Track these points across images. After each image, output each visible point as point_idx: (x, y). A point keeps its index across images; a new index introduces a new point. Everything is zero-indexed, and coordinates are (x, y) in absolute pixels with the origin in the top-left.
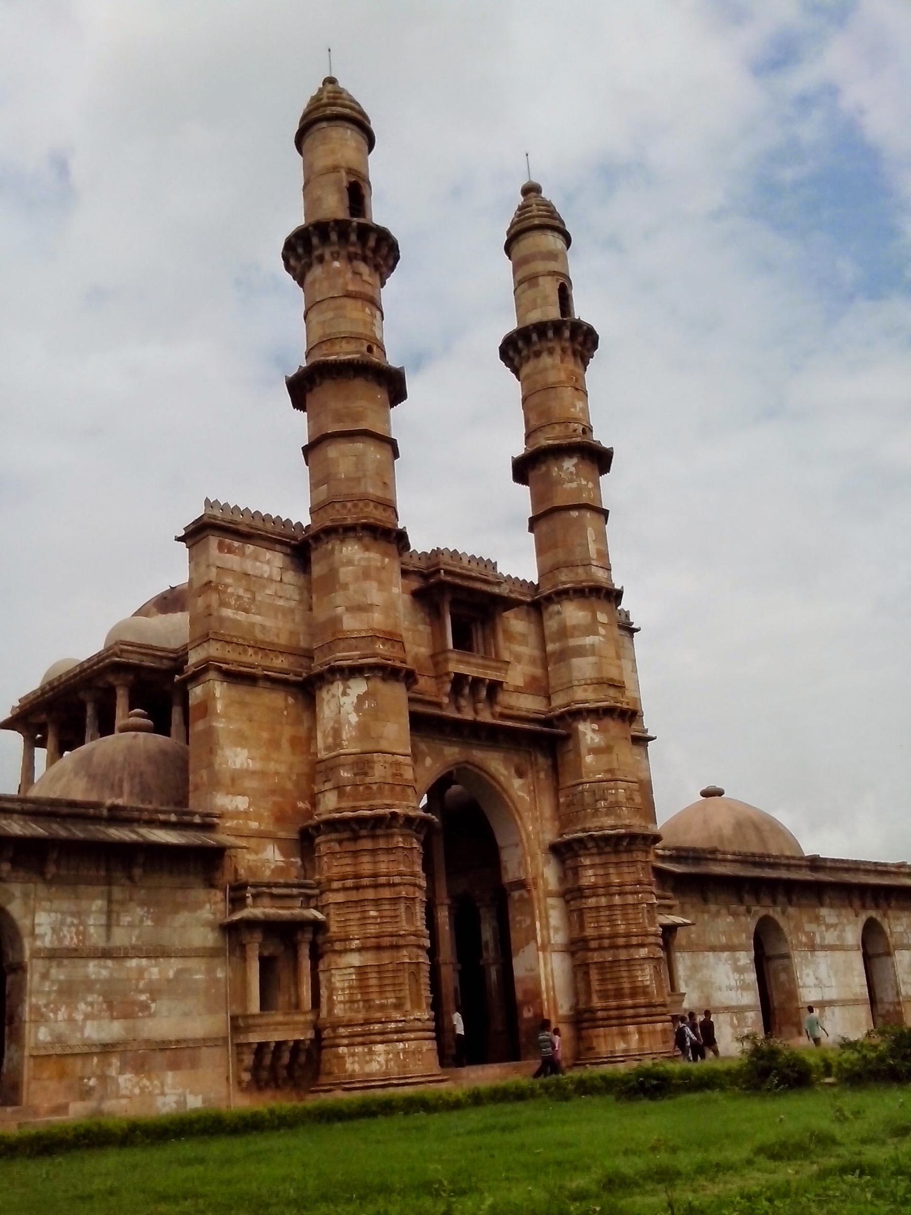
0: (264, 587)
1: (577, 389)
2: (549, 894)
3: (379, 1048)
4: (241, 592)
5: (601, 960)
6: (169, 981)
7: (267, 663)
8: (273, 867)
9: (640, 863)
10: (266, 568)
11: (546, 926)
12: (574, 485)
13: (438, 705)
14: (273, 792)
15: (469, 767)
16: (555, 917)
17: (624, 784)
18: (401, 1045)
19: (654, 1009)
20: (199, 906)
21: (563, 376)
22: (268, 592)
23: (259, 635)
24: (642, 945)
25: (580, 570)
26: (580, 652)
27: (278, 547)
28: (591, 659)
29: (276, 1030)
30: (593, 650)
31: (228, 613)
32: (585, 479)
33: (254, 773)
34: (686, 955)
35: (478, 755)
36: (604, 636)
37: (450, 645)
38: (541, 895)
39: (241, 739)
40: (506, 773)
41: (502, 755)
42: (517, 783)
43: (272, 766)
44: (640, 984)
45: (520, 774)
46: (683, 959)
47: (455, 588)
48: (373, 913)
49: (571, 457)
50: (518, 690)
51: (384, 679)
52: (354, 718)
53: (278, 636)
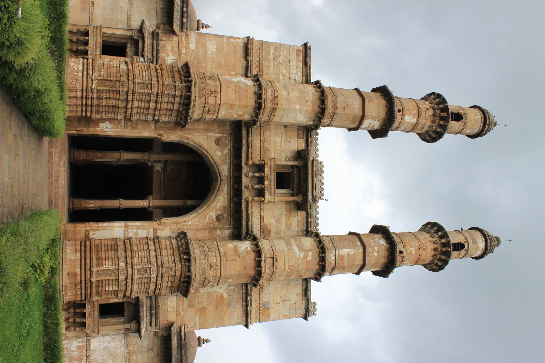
0: (286, 70)
1: (420, 249)
2: (155, 230)
3: (81, 67)
4: (282, 58)
5: (119, 249)
6: (118, 3)
7: (254, 66)
8: (166, 58)
9: (174, 265)
10: (294, 72)
11: (138, 228)
12: (373, 244)
13: (247, 159)
14: (199, 63)
15: (219, 182)
16: (142, 234)
17: (219, 263)
18: (81, 74)
19: (88, 267)
20: (149, 21)
21: (423, 242)
22: (284, 71)
23: (265, 64)
24: (126, 266)
25: (331, 245)
26: (288, 243)
27: (304, 78)
28: (285, 248)
29: (94, 40)
30: (290, 249)
31: (272, 51)
32: (378, 249)
33: (206, 53)
34: (123, 349)
36: (299, 256)
37: (277, 163)
38: (154, 227)
39: (220, 49)
40: (218, 207)
41: (226, 204)
42: (213, 215)
43: (210, 63)
44: (104, 263)
45: (218, 218)
46: (120, 347)
47: (306, 166)
48: (144, 73)
49: (386, 243)
50: (262, 218)
51: (255, 93)
52: (235, 80)
53: (266, 74)
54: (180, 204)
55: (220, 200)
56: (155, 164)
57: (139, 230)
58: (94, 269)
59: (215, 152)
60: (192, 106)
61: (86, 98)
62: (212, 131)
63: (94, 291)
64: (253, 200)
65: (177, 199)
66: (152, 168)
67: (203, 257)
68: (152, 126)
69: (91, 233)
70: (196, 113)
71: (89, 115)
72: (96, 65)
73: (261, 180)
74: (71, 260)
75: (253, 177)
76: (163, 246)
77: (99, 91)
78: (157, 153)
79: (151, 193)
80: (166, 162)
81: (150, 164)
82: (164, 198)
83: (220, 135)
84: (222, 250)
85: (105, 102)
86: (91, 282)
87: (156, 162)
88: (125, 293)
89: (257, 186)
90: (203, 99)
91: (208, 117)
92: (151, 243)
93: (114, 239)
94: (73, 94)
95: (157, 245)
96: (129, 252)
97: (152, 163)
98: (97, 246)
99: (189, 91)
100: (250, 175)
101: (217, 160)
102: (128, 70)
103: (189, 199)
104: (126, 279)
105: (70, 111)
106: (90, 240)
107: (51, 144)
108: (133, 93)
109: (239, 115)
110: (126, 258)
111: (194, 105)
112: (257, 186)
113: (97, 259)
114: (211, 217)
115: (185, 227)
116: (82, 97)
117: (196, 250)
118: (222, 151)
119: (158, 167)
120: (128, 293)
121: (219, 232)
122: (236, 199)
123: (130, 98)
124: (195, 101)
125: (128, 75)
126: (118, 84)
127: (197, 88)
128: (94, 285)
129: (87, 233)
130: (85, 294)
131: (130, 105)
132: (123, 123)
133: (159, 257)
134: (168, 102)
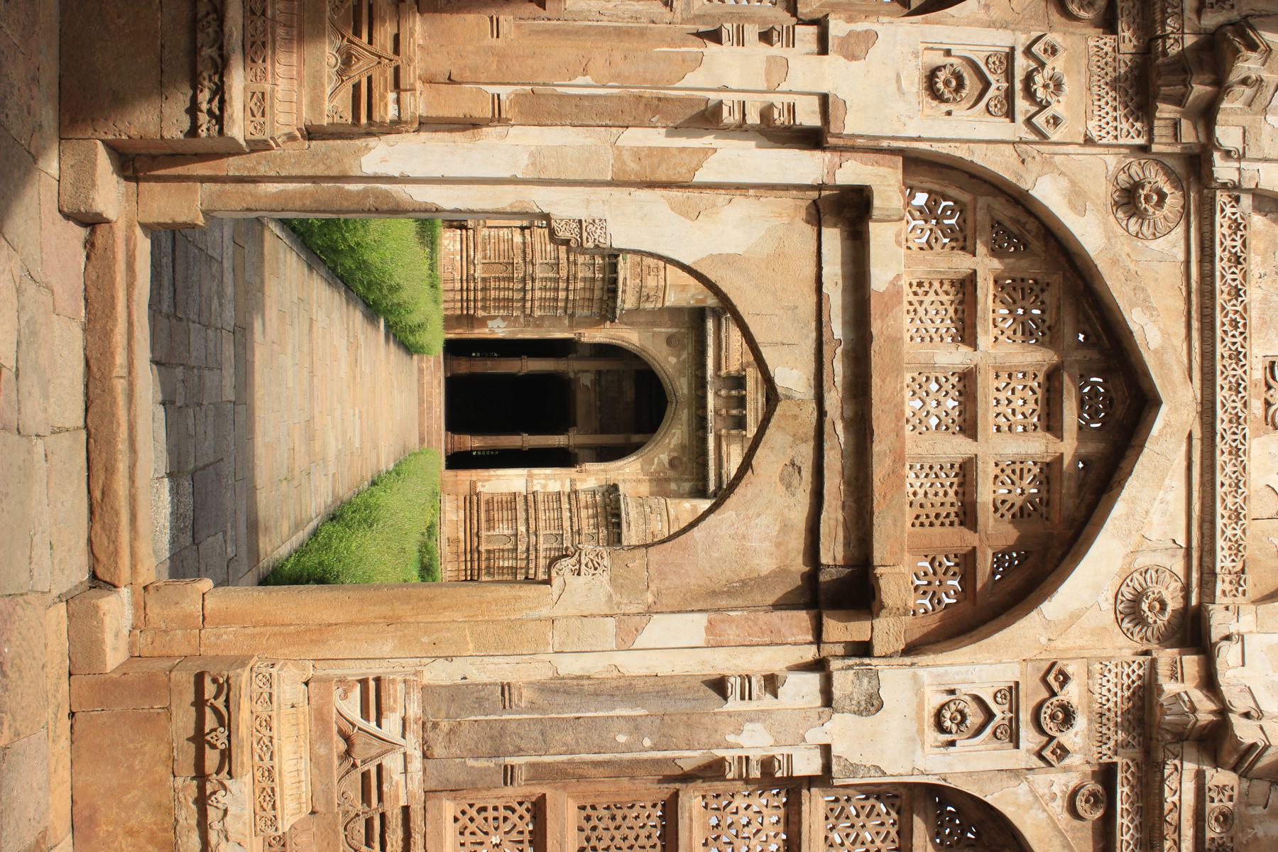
11: (547, 477)
16: (554, 487)
18: (458, 258)
24: (528, 530)
35: (684, 415)
42: (665, 458)
45: (672, 463)
54: (619, 441)
55: (674, 436)
56: (580, 375)
57: (549, 480)
58: (483, 533)
59: (666, 358)
60: (620, 293)
61: (468, 289)
62: (660, 325)
63: (483, 565)
64: (729, 435)
65: (618, 433)
66: (577, 380)
67: (641, 521)
68: (566, 322)
69: (479, 484)
70: (627, 300)
71: (472, 312)
72: (479, 240)
73: (741, 402)
74: (451, 521)
75: (729, 397)
76: (582, 504)
77: (484, 280)
78: (583, 358)
79: (575, 425)
80: (599, 373)
81: (572, 375)
82: (596, 433)
83: (675, 330)
84: (672, 511)
85: (493, 294)
86: (479, 552)
87: (582, 372)
88: (527, 573)
89: (734, 412)
90: (638, 281)
91: (649, 306)
92: (564, 499)
93: (510, 494)
94: (449, 286)
95: (574, 502)
96: (532, 511)
97: (576, 373)
98: (487, 503)
99: (616, 272)
100: (723, 393)
101: (670, 371)
102: (524, 243)
103: (638, 432)
104: (528, 549)
105: (446, 309)
106: (477, 495)
107: (421, 361)
108: (533, 280)
109: (697, 301)
110: (527, 519)
111: (624, 291)
112: (734, 412)
113: (488, 521)
114: (660, 462)
115: (620, 477)
116: (462, 290)
117: (630, 511)
118: (678, 356)
119: (586, 380)
120: (532, 571)
121: (673, 486)
122: (700, 433)
123: (529, 287)
124: (625, 284)
125: (524, 252)
126: (510, 268)
127: (628, 265)
128: (484, 556)
129: (473, 485)
130: (472, 569)
131: (529, 296)
132: (522, 320)
133: (575, 519)
134: (584, 289)
